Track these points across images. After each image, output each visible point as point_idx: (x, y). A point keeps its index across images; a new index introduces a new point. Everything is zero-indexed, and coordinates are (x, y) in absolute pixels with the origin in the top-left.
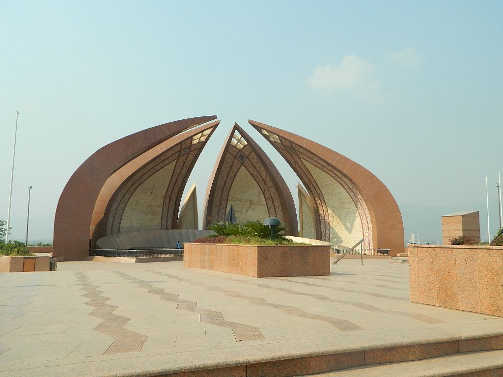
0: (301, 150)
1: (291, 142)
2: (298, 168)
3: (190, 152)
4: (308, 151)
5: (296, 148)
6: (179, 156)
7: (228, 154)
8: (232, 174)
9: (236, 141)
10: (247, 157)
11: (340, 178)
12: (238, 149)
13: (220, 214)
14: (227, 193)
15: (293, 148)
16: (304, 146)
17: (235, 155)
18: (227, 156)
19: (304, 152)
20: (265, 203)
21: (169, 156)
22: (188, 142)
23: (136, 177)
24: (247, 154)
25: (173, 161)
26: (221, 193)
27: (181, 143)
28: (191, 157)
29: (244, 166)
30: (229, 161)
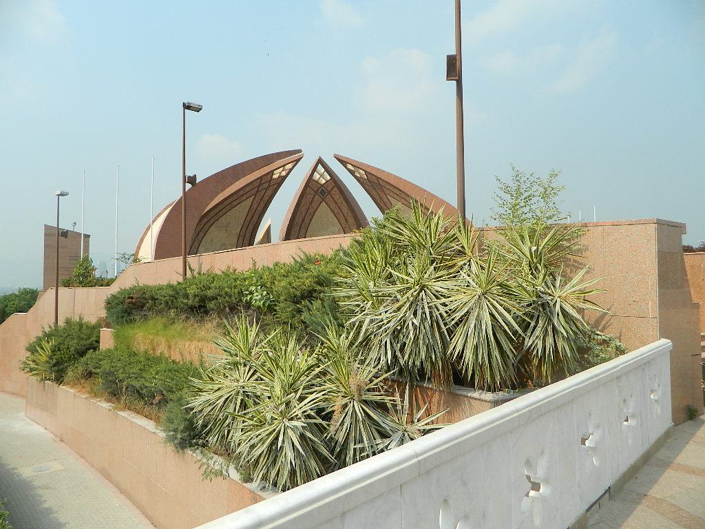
0: (388, 186)
1: (378, 178)
2: (382, 205)
3: (269, 186)
4: (395, 187)
7: (309, 189)
8: (311, 210)
9: (318, 176)
10: (329, 193)
16: (392, 182)
19: (391, 188)
22: (269, 176)
23: (212, 214)
24: (329, 189)
27: (261, 178)
28: (269, 192)
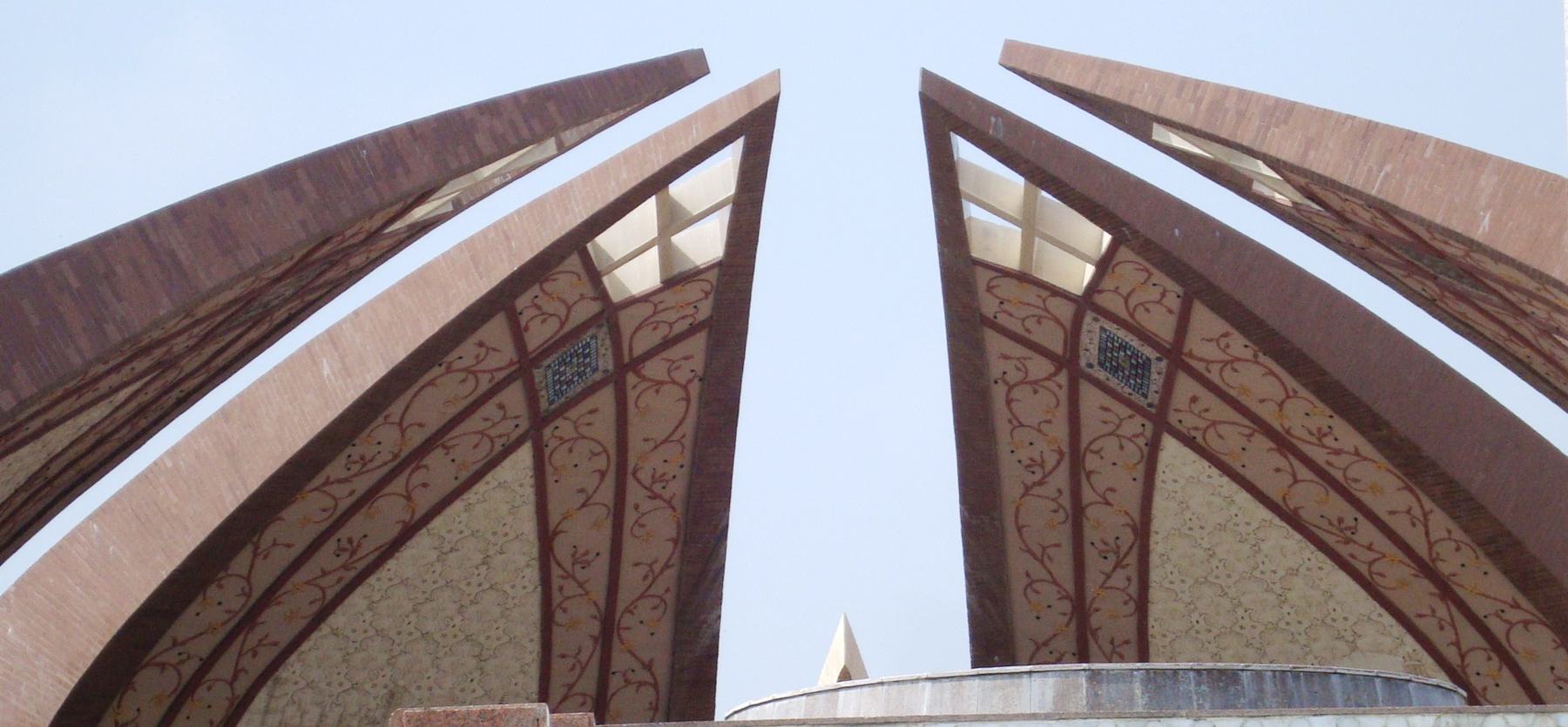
3: (626, 366)
5: (1455, 250)
6: (540, 419)
7: (995, 344)
8: (1107, 525)
10: (1176, 355)
12: (1056, 292)
15: (1441, 255)
16: (1481, 231)
17: (1056, 344)
18: (996, 367)
21: (434, 422)
22: (566, 282)
24: (1162, 324)
25: (492, 464)
29: (1188, 441)
30: (1031, 406)
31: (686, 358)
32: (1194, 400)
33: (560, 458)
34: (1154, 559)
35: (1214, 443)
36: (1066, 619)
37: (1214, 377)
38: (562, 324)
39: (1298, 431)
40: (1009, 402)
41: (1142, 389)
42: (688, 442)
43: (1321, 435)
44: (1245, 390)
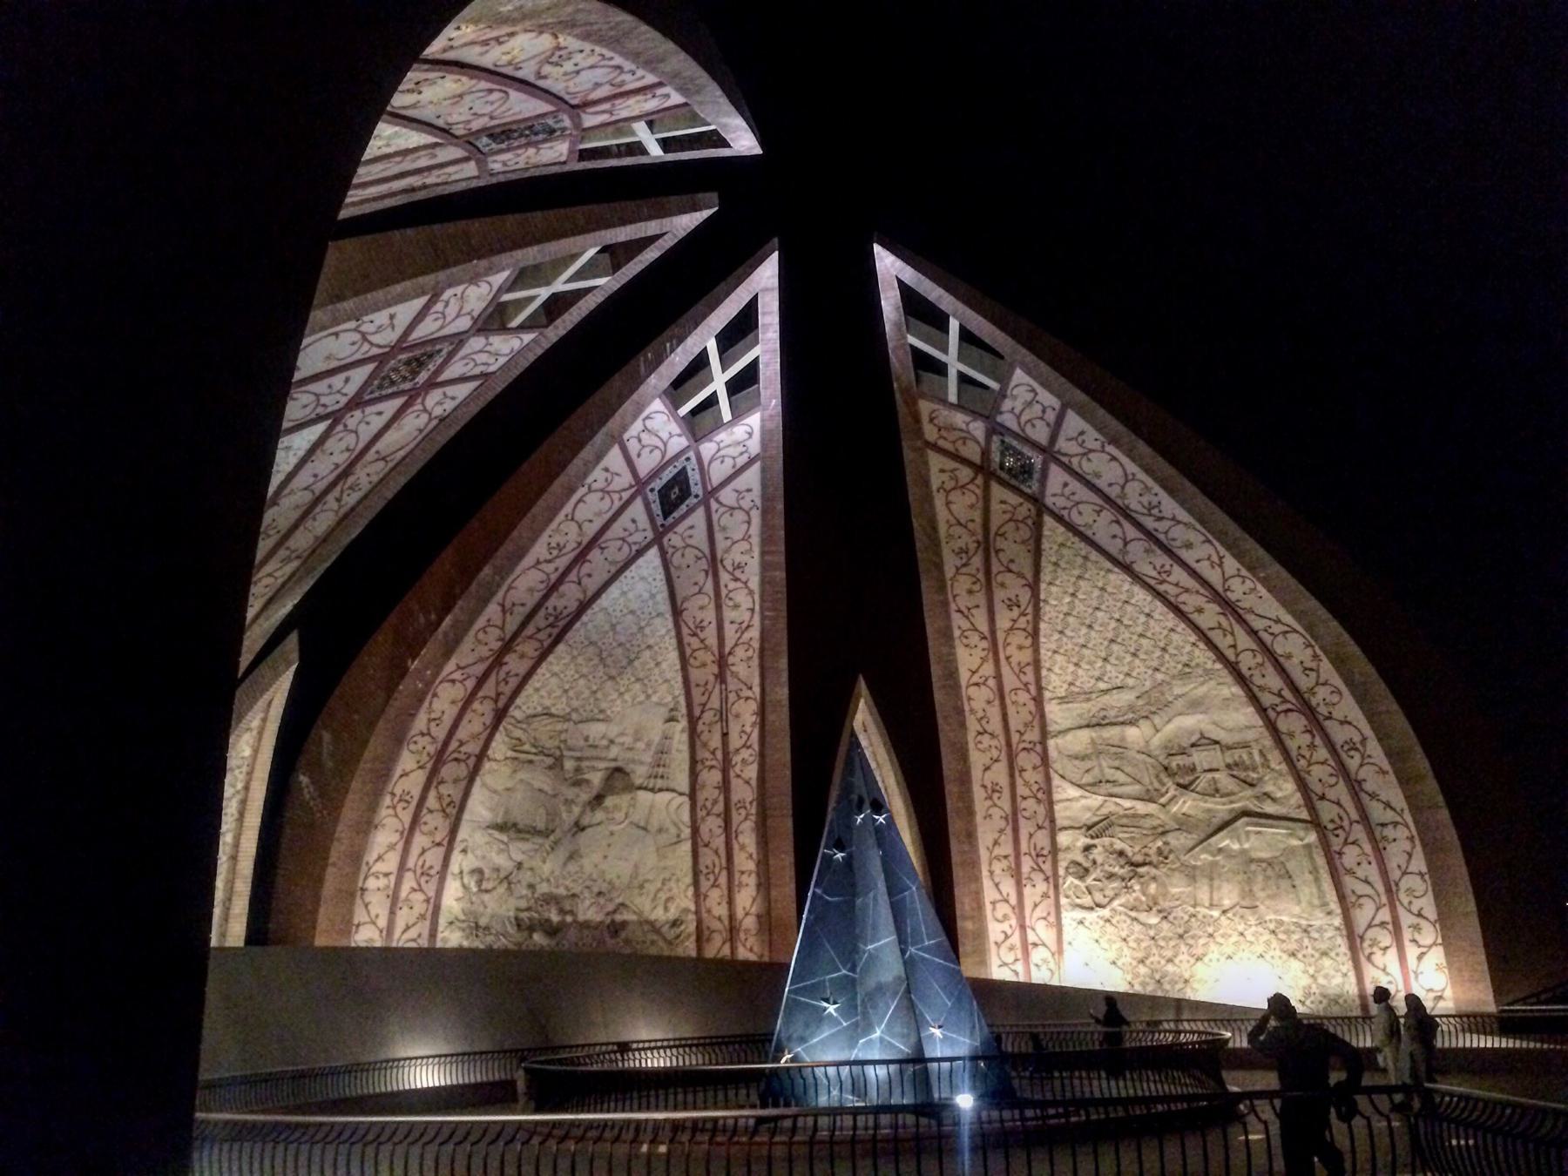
3: (432, 384)
8: (570, 595)
10: (711, 493)
11: (1253, 633)
13: (415, 850)
14: (488, 719)
18: (598, 475)
20: (683, 782)
24: (717, 473)
26: (451, 712)
29: (663, 553)
31: (453, 398)
32: (692, 527)
33: (330, 444)
34: (578, 625)
35: (676, 560)
36: (488, 654)
37: (715, 517)
38: (442, 327)
39: (728, 563)
40: (580, 501)
41: (666, 515)
42: (391, 465)
43: (739, 567)
44: (724, 529)
